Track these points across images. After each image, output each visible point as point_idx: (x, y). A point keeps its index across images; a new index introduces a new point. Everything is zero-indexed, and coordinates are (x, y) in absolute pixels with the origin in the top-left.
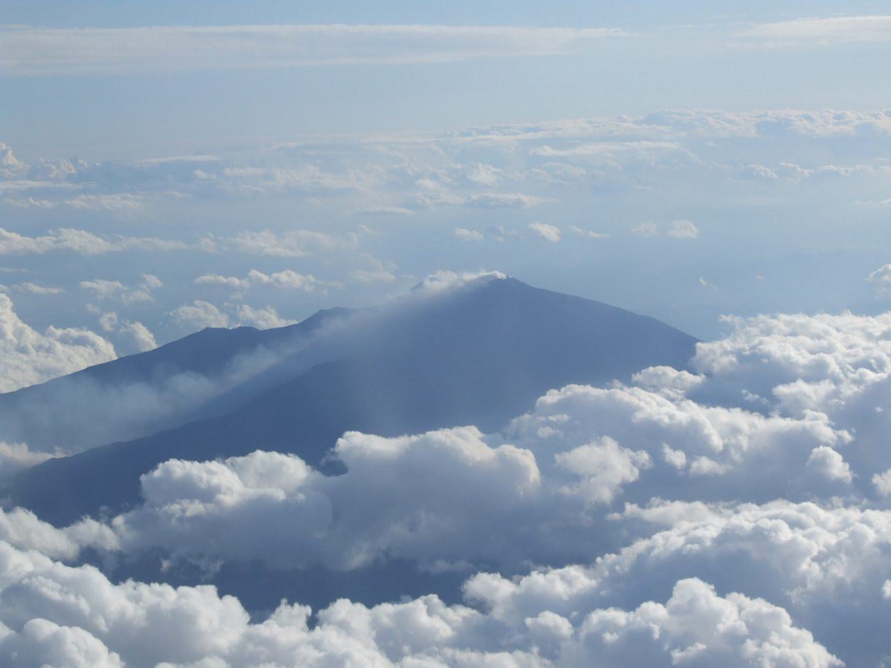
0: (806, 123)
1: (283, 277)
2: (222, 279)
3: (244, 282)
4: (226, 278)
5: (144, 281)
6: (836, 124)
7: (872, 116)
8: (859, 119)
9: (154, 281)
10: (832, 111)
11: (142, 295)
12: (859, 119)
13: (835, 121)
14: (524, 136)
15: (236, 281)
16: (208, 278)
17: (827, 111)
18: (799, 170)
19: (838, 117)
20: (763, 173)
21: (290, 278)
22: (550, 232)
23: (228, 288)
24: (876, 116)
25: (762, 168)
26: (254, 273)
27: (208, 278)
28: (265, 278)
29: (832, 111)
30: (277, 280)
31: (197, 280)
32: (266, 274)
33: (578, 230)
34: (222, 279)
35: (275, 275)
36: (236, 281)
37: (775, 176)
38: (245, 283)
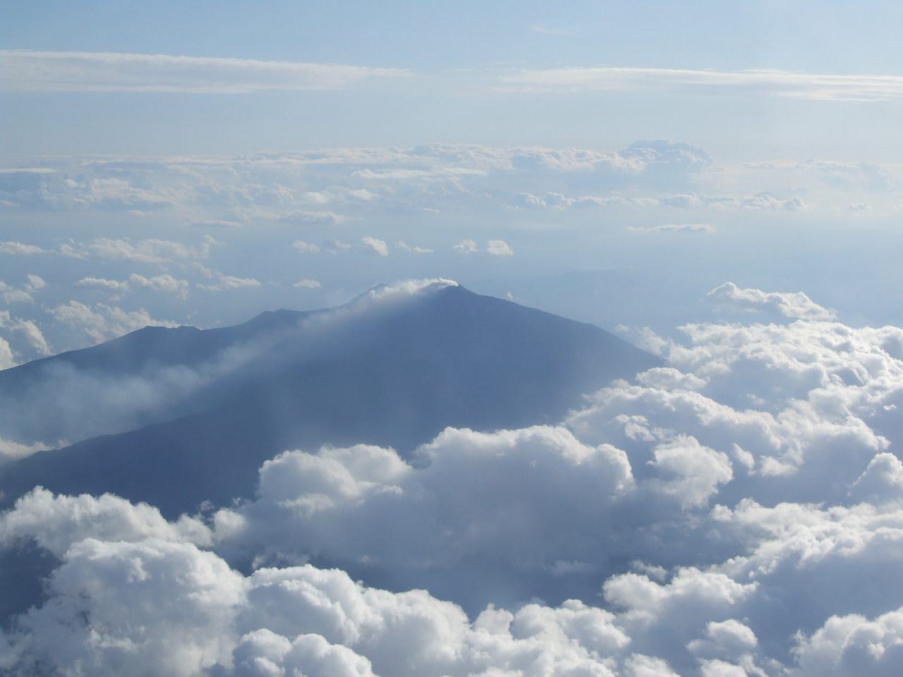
1: (162, 280)
2: (104, 281)
3: (122, 285)
4: (108, 280)
5: (27, 281)
8: (598, 158)
9: (38, 281)
10: (575, 150)
11: (23, 296)
12: (598, 158)
15: (116, 284)
17: (572, 150)
18: (563, 199)
19: (581, 156)
20: (534, 202)
21: (166, 281)
22: (380, 246)
23: (109, 290)
24: (612, 155)
25: (532, 196)
26: (135, 276)
28: (145, 281)
29: (575, 150)
30: (157, 284)
31: (82, 281)
32: (146, 278)
33: (404, 245)
34: (104, 281)
35: (155, 279)
36: (116, 284)
37: (544, 203)
38: (124, 285)
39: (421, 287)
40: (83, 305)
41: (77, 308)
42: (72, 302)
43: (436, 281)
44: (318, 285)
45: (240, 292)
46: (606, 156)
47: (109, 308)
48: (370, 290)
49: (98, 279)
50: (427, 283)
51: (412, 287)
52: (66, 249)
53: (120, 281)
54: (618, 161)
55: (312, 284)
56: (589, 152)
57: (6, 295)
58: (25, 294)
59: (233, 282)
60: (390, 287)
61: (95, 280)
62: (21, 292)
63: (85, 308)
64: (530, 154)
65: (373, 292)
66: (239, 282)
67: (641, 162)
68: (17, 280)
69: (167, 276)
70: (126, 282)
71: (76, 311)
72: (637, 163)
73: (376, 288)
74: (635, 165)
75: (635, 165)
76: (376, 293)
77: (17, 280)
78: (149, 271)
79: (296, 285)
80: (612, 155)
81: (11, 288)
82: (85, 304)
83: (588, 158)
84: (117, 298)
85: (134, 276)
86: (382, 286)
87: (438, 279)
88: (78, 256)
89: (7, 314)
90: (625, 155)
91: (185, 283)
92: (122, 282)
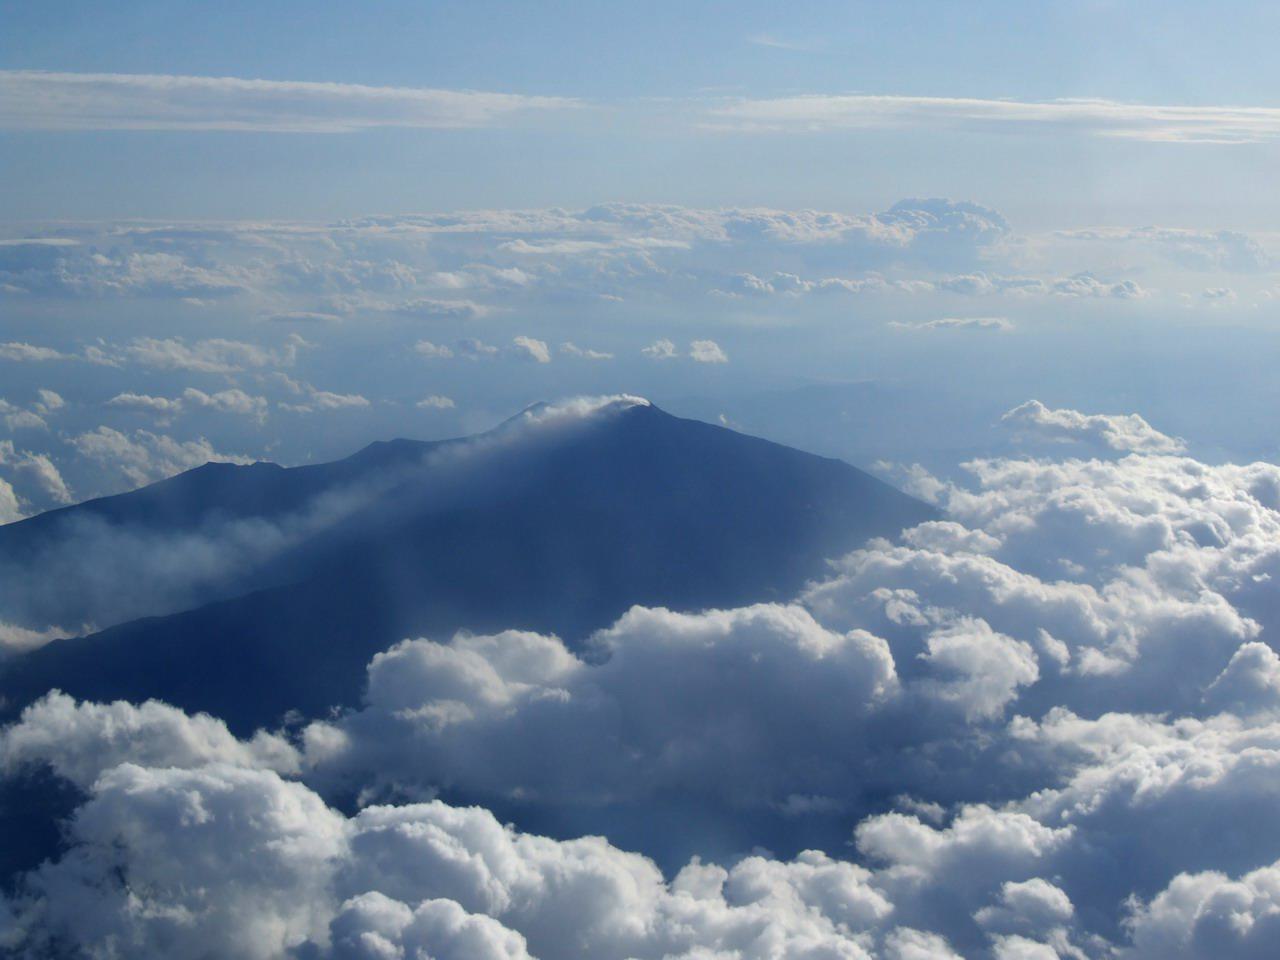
0: (784, 225)
2: (148, 399)
3: (172, 403)
5: (38, 398)
6: (820, 229)
7: (862, 220)
8: (847, 223)
9: (53, 399)
12: (847, 223)
13: (820, 225)
14: (436, 229)
15: (164, 403)
16: (126, 397)
19: (823, 221)
24: (868, 221)
27: (126, 397)
31: (116, 399)
34: (148, 399)
36: (164, 403)
38: (176, 404)
39: (597, 406)
40: (117, 433)
41: (109, 436)
42: (103, 428)
43: (618, 398)
44: (451, 403)
45: (341, 413)
46: (859, 221)
47: (155, 437)
48: (525, 411)
49: (139, 395)
50: (605, 401)
51: (585, 407)
52: (94, 354)
53: (170, 397)
54: (876, 229)
55: (443, 403)
56: (834, 215)
57: (9, 418)
58: (35, 416)
59: (329, 399)
60: (552, 407)
61: (134, 397)
62: (30, 414)
63: (120, 436)
64: (751, 219)
65: (529, 414)
66: (338, 401)
67: (908, 230)
68: (25, 398)
69: (237, 391)
70: (178, 400)
71: (105, 441)
72: (903, 231)
73: (532, 409)
74: (900, 234)
75: (900, 234)
76: (534, 415)
77: (25, 398)
78: (212, 384)
79: (419, 404)
80: (868, 221)
81: (15, 408)
82: (121, 431)
83: (833, 223)
84: (166, 423)
85: (191, 392)
86: (542, 405)
87: (621, 396)
88: (111, 363)
89: (10, 445)
90: (886, 220)
91: (263, 401)
92: (173, 399)
